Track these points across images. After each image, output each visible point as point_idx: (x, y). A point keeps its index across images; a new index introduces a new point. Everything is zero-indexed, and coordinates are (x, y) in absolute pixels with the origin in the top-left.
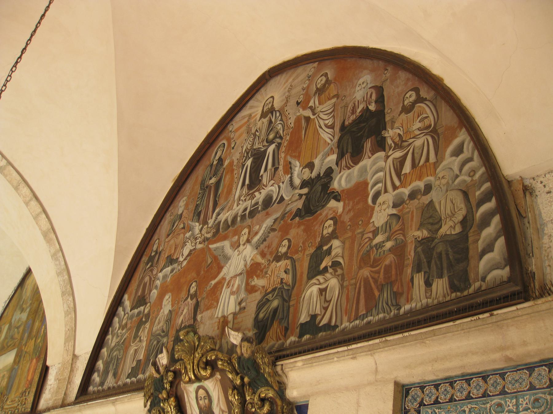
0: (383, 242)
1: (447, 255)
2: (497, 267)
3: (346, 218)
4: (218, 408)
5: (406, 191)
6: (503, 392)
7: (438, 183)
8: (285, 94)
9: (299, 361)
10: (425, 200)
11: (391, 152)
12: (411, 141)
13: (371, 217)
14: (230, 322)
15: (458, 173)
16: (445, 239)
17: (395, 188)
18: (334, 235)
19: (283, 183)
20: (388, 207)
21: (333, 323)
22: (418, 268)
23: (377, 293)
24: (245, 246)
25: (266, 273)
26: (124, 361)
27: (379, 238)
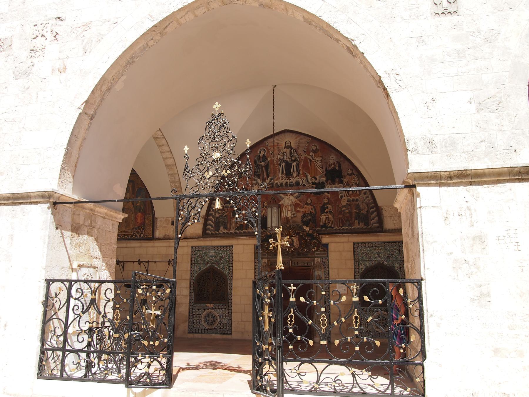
0: (345, 210)
1: (363, 218)
3: (332, 200)
4: (296, 244)
5: (351, 199)
6: (376, 246)
7: (360, 200)
8: (296, 143)
9: (327, 236)
10: (357, 203)
11: (345, 186)
12: (351, 185)
13: (341, 202)
14: (290, 219)
15: (365, 199)
17: (347, 197)
18: (328, 203)
19: (304, 179)
20: (346, 201)
21: (332, 227)
23: (345, 222)
24: (290, 196)
26: (230, 224)
27: (344, 209)
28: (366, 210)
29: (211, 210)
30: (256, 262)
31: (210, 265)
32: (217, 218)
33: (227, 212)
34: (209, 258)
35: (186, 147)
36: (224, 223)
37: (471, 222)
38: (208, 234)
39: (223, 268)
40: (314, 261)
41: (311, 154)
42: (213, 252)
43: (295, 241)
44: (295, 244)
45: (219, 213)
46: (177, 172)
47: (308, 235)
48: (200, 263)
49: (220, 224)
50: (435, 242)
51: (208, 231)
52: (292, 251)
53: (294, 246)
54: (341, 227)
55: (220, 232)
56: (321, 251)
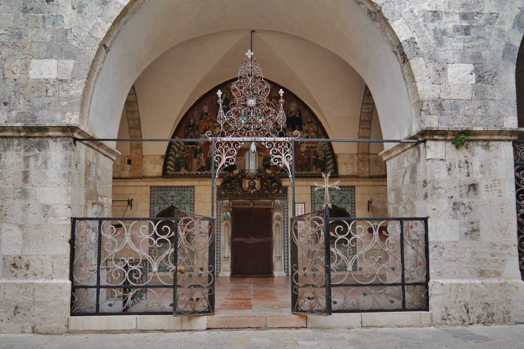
2: (331, 169)
5: (310, 145)
10: (315, 150)
13: (300, 148)
16: (320, 160)
22: (314, 165)
23: (303, 167)
25: (265, 152)
27: (303, 155)
28: (323, 156)
29: (171, 150)
30: (217, 203)
31: (170, 205)
32: (178, 159)
33: (187, 153)
34: (170, 198)
35: (219, 91)
36: (185, 164)
37: (468, 173)
38: (169, 174)
39: (185, 209)
40: (274, 202)
41: (273, 100)
42: (174, 192)
43: (257, 183)
44: (256, 187)
45: (179, 154)
46: (137, 109)
47: (270, 178)
48: (159, 204)
49: (181, 165)
50: (440, 188)
51: (168, 172)
52: (254, 192)
53: (255, 188)
54: (300, 172)
55: (181, 172)
56: (281, 194)
